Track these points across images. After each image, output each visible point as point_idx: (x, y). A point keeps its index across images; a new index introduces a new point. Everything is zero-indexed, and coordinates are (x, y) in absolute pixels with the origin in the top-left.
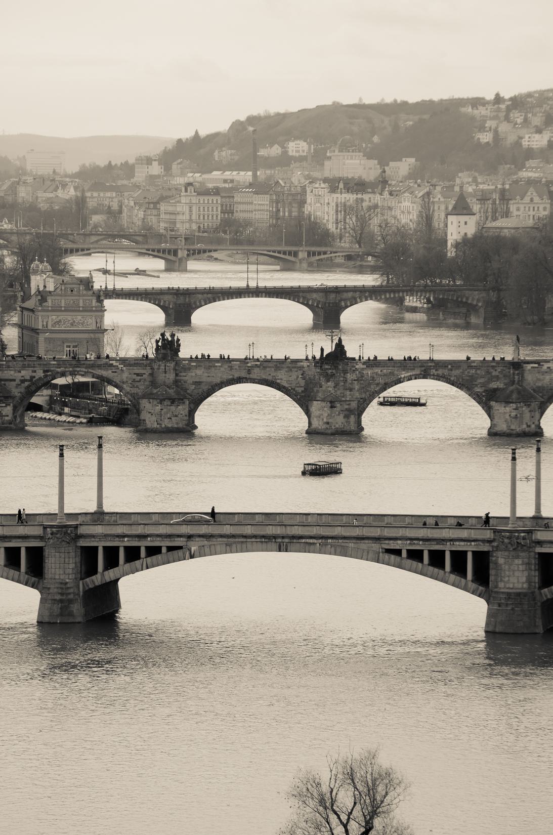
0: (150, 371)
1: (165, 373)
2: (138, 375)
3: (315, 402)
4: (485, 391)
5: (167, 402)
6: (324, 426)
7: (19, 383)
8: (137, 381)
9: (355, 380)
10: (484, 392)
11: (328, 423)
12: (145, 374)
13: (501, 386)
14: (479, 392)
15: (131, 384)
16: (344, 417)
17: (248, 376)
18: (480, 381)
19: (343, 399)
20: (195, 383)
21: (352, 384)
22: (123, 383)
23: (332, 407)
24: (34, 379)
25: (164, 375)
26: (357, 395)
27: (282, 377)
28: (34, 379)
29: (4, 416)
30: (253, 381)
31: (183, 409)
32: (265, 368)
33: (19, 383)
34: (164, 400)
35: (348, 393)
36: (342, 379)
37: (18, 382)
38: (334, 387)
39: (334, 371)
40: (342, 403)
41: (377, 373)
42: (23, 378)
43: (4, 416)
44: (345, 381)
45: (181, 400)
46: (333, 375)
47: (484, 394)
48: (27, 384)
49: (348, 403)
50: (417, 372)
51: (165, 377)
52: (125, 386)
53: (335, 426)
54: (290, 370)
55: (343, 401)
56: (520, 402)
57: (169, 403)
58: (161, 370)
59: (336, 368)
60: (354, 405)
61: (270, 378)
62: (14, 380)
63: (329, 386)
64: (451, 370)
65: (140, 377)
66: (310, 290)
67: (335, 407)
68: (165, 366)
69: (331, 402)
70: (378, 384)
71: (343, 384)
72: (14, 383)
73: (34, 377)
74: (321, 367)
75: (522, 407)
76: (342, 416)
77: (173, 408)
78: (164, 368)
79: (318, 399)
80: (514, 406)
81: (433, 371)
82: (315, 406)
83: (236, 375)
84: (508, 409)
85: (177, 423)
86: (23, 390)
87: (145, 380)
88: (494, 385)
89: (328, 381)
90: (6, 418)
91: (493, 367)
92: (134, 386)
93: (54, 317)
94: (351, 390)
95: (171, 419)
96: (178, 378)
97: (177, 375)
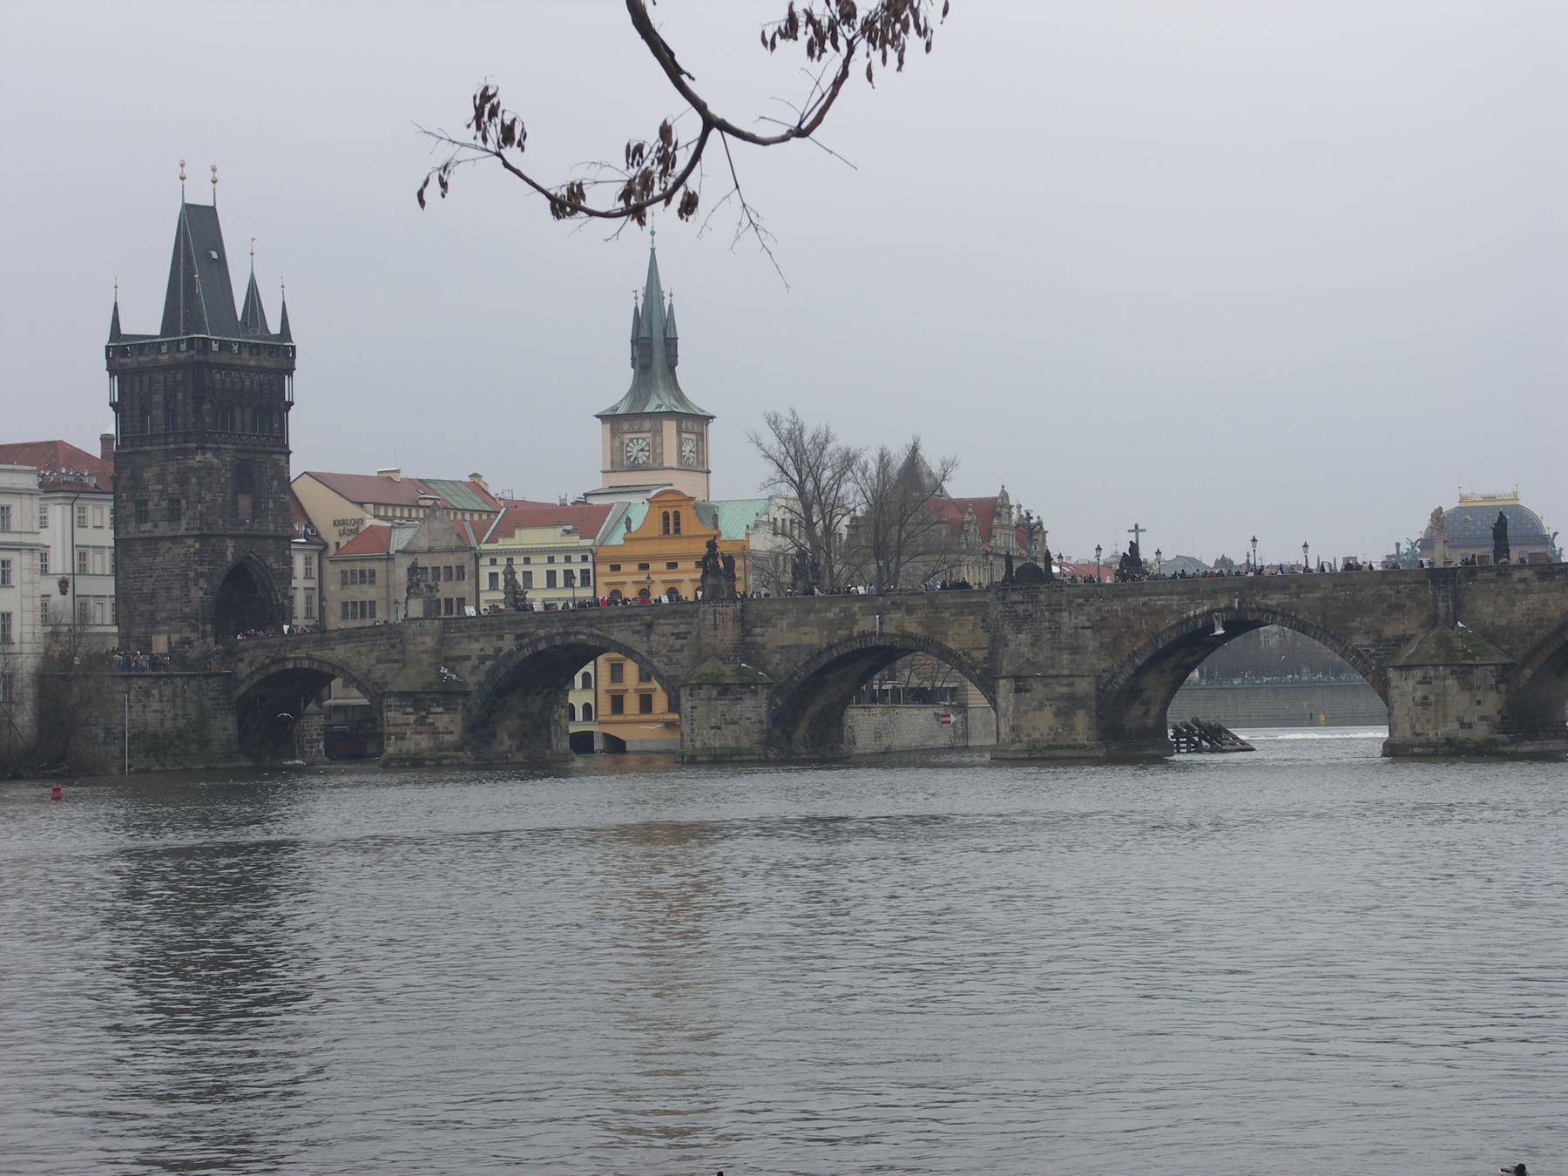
1: (716, 629)
3: (1002, 682)
7: (477, 663)
8: (677, 651)
9: (1083, 628)
10: (1373, 646)
12: (690, 633)
14: (1362, 646)
15: (667, 656)
19: (1051, 672)
22: (651, 653)
23: (1018, 690)
24: (501, 654)
25: (713, 633)
28: (501, 654)
29: (443, 733)
33: (477, 663)
34: (700, 686)
35: (1066, 658)
36: (1046, 624)
37: (474, 661)
38: (1032, 644)
39: (1030, 607)
40: (1049, 681)
42: (482, 653)
43: (443, 733)
44: (1056, 629)
46: (1028, 617)
47: (1372, 651)
48: (489, 663)
49: (1065, 681)
51: (716, 636)
53: (1029, 735)
55: (1053, 676)
56: (1436, 666)
57: (714, 693)
58: (707, 623)
59: (1034, 599)
60: (1084, 686)
62: (467, 658)
63: (1019, 642)
65: (681, 642)
67: (1027, 691)
68: (715, 612)
69: (1016, 678)
71: (1049, 636)
72: (468, 665)
73: (501, 650)
74: (1004, 598)
75: (1444, 678)
78: (712, 616)
79: (1004, 673)
80: (1418, 673)
84: (1411, 683)
85: (737, 739)
86: (482, 677)
89: (1019, 631)
90: (447, 737)
92: (671, 660)
94: (1074, 650)
95: (719, 728)
96: (749, 639)
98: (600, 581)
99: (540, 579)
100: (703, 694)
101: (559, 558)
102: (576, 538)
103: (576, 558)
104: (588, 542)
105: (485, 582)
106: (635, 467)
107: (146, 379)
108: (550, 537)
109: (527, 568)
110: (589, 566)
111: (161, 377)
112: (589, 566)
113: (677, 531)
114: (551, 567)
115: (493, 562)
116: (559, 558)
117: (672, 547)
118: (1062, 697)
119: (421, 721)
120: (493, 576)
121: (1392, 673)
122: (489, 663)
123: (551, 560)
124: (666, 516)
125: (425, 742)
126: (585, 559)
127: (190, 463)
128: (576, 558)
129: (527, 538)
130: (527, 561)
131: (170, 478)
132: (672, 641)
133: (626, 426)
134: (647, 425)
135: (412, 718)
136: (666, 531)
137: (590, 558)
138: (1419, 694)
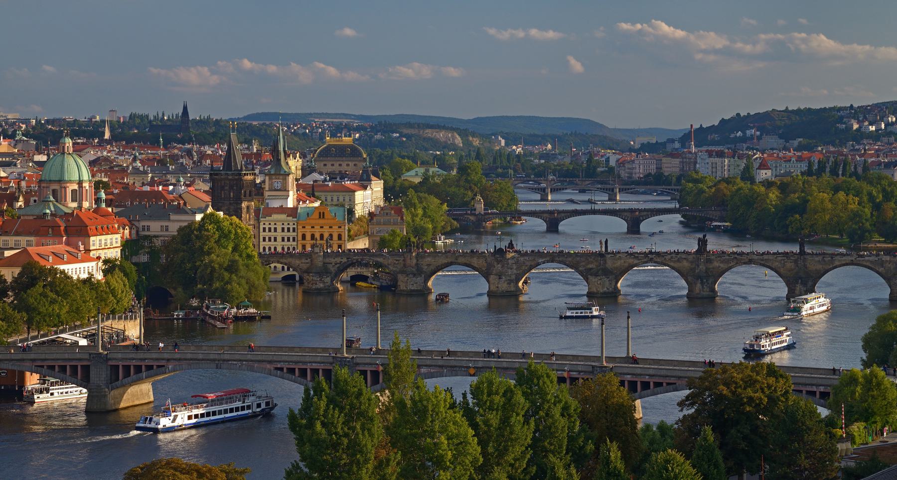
0: (402, 259)
2: (397, 260)
4: (585, 269)
5: (411, 276)
6: (496, 289)
11: (498, 287)
13: (594, 267)
16: (508, 284)
17: (456, 261)
18: (583, 264)
20: (429, 265)
21: (512, 265)
22: (389, 264)
26: (515, 271)
27: (475, 261)
30: (459, 264)
31: (420, 280)
32: (465, 257)
35: (510, 270)
41: (526, 260)
44: (508, 264)
45: (420, 275)
48: (338, 265)
50: (548, 259)
52: (390, 267)
54: (478, 258)
60: (513, 277)
61: (468, 262)
64: (566, 258)
66: (625, 210)
70: (527, 266)
76: (506, 283)
77: (414, 279)
81: (557, 259)
82: (492, 277)
83: (450, 261)
87: (401, 263)
88: (590, 266)
89: (498, 264)
91: (589, 256)
93: (377, 228)
94: (511, 269)
97: (417, 260)
98: (299, 231)
99: (279, 230)
100: (411, 276)
101: (286, 224)
102: (291, 218)
103: (291, 224)
104: (296, 219)
105: (261, 230)
106: (276, 190)
107: (223, 182)
108: (283, 217)
109: (275, 226)
110: (295, 226)
111: (228, 182)
112: (295, 226)
113: (323, 217)
114: (283, 226)
115: (264, 224)
116: (286, 224)
117: (322, 221)
118: (509, 280)
119: (321, 280)
120: (264, 229)
121: (589, 276)
122: (338, 265)
123: (283, 224)
124: (320, 213)
125: (322, 285)
126: (294, 224)
127: (239, 206)
128: (291, 224)
129: (275, 217)
130: (275, 224)
131: (231, 210)
132: (395, 261)
133: (274, 177)
134: (281, 177)
135: (318, 279)
136: (320, 217)
137: (296, 224)
138: (599, 282)
